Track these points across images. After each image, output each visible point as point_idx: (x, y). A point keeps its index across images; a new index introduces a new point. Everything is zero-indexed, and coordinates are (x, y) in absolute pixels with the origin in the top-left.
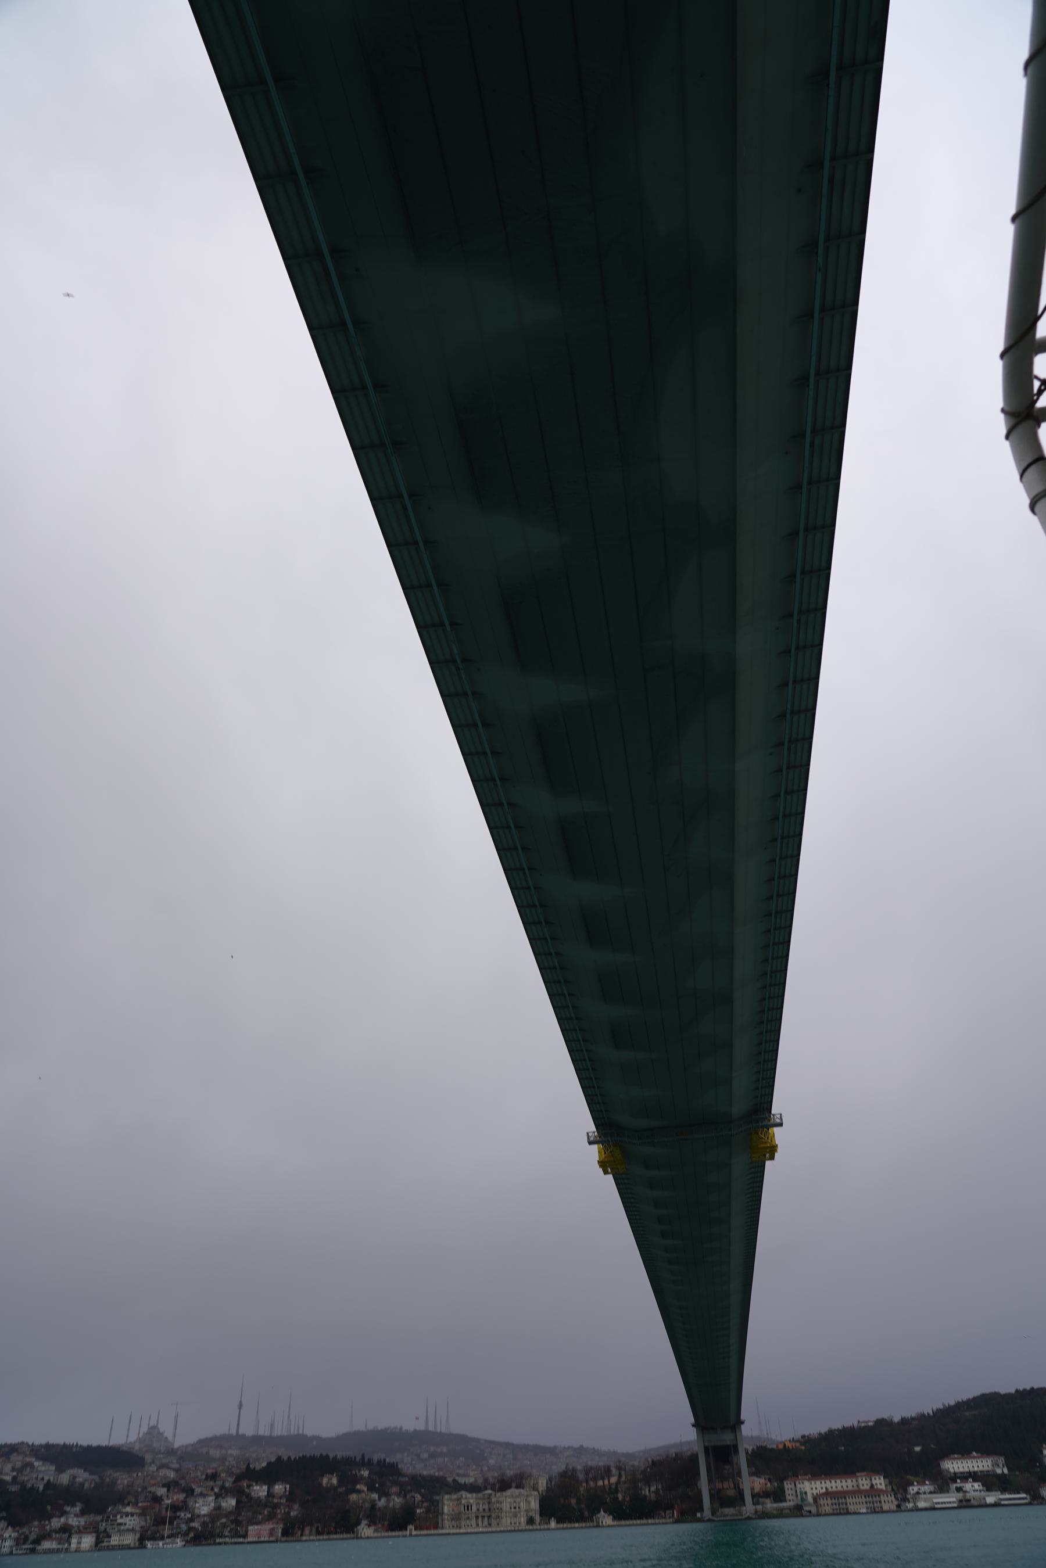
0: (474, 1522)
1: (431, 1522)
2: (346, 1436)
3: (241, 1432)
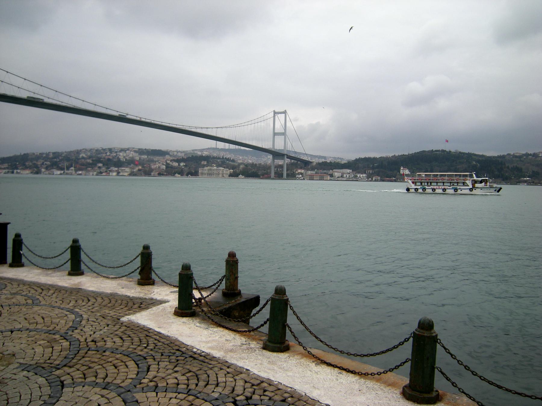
1: (195, 174)
3: (217, 147)
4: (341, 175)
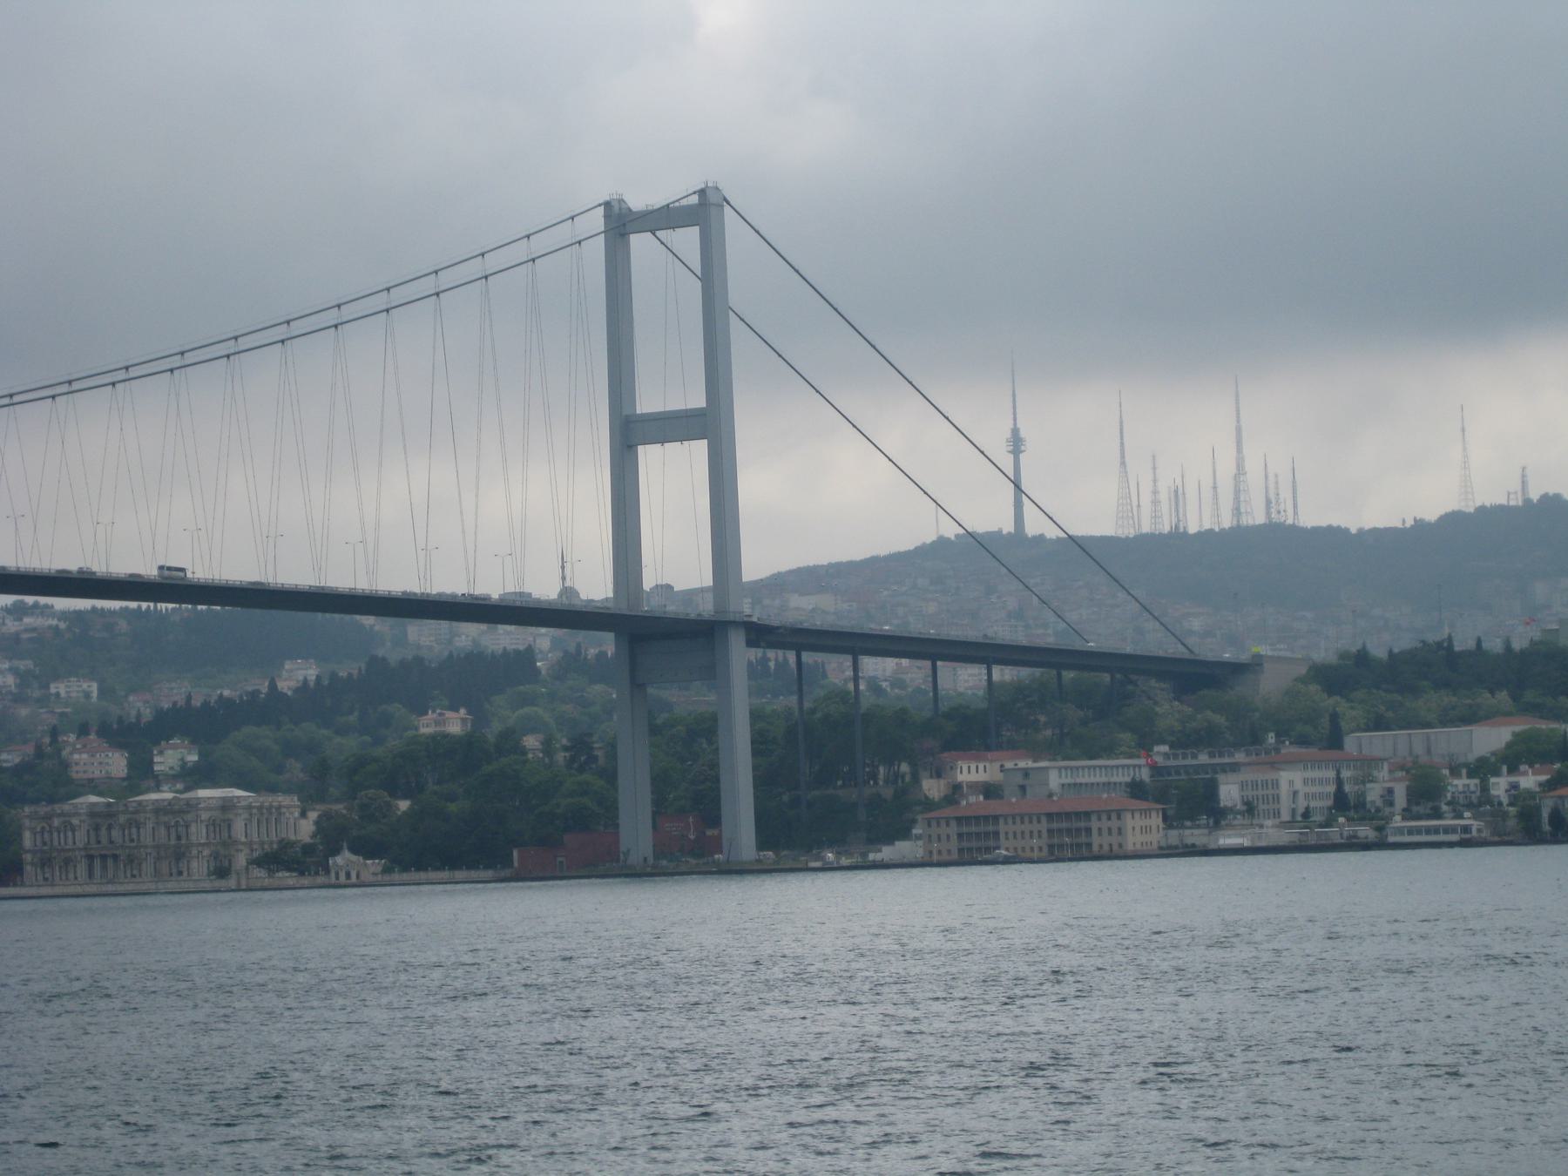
0: (82, 869)
2: (1453, 520)
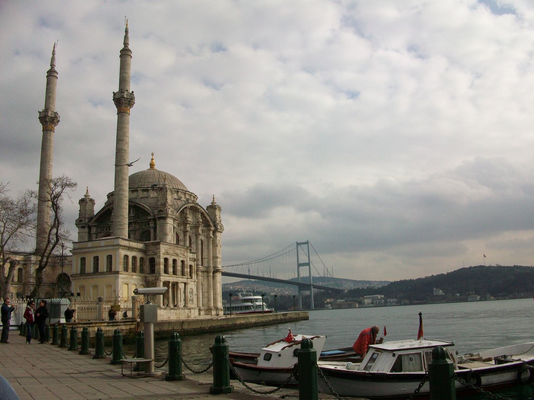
4: (371, 301)
